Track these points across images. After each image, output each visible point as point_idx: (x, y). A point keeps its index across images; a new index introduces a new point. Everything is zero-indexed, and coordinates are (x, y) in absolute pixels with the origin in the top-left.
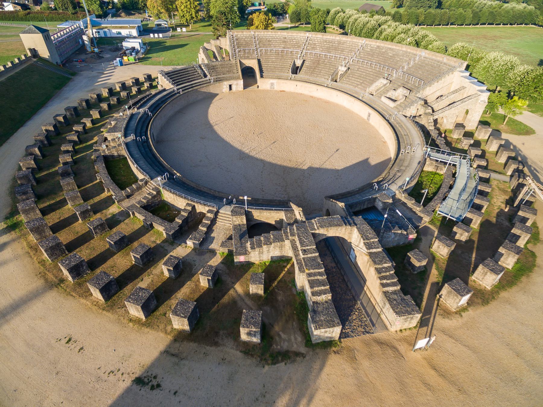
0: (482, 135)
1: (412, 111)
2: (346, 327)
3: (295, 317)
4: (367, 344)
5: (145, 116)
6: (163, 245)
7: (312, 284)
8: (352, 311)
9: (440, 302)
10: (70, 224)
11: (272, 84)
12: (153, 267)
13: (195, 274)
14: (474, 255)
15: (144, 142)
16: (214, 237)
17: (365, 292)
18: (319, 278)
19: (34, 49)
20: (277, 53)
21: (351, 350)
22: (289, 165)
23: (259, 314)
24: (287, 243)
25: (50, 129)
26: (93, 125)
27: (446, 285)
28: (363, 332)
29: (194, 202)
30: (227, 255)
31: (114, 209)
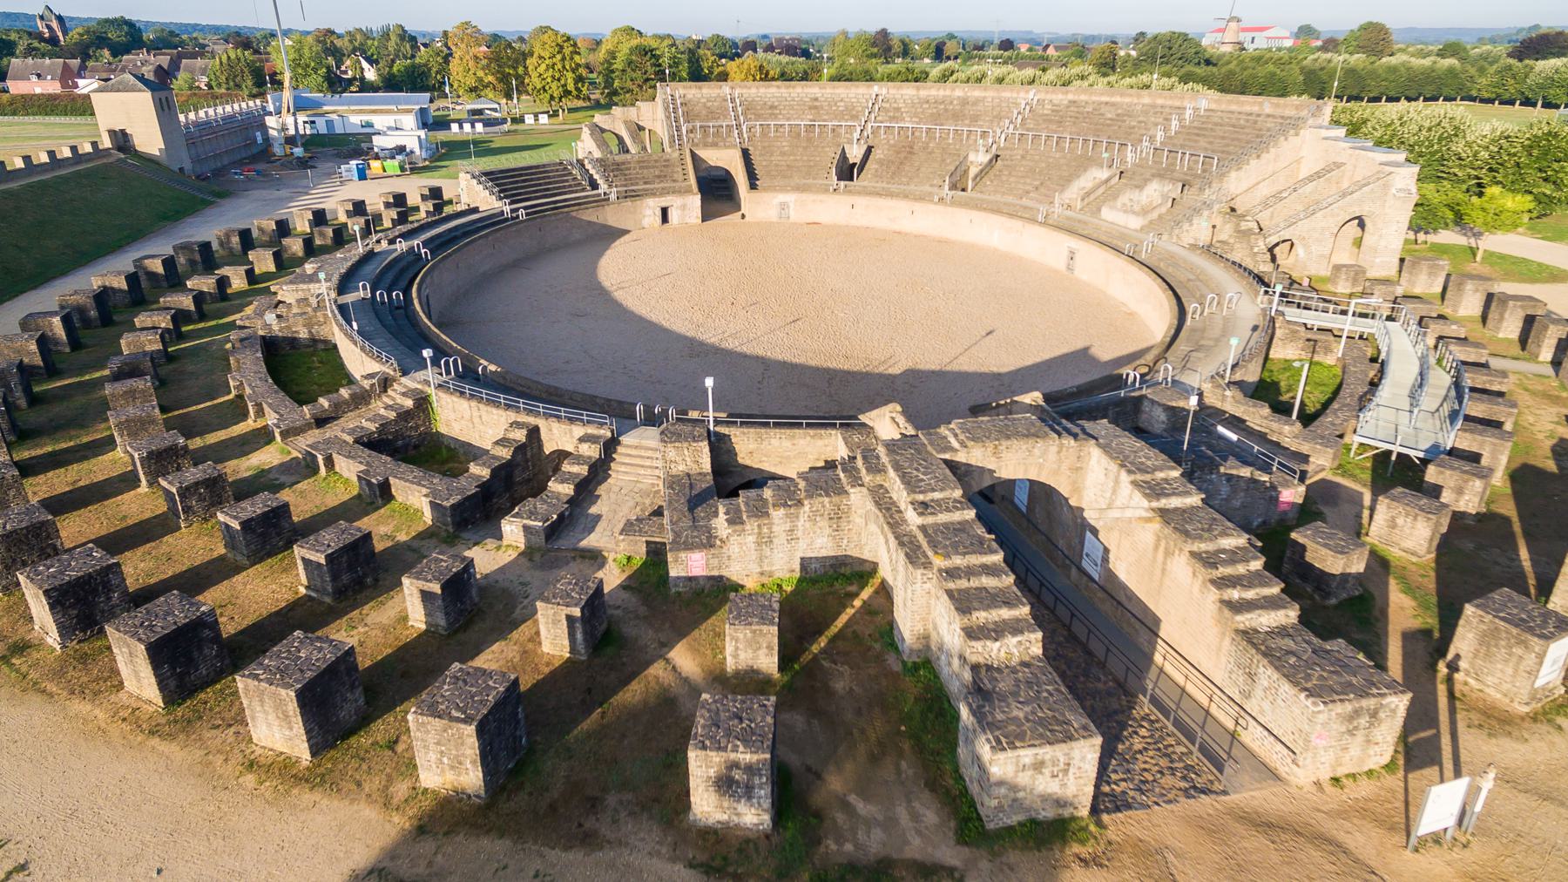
1: (1199, 230)
2: (1114, 776)
3: (906, 746)
4: (1210, 829)
5: (411, 258)
6: (415, 544)
7: (963, 602)
8: (1124, 726)
9: (1458, 688)
10: (107, 497)
12: (371, 604)
13: (525, 621)
14: (1524, 554)
15: (397, 308)
16: (598, 517)
17: (1161, 670)
18: (988, 582)
19: (123, 131)
20: (795, 132)
21: (1147, 853)
23: (765, 706)
24: (859, 500)
25: (115, 285)
26: (250, 284)
27: (1469, 609)
28: (1186, 791)
29: (537, 414)
30: (644, 563)
31: (267, 457)
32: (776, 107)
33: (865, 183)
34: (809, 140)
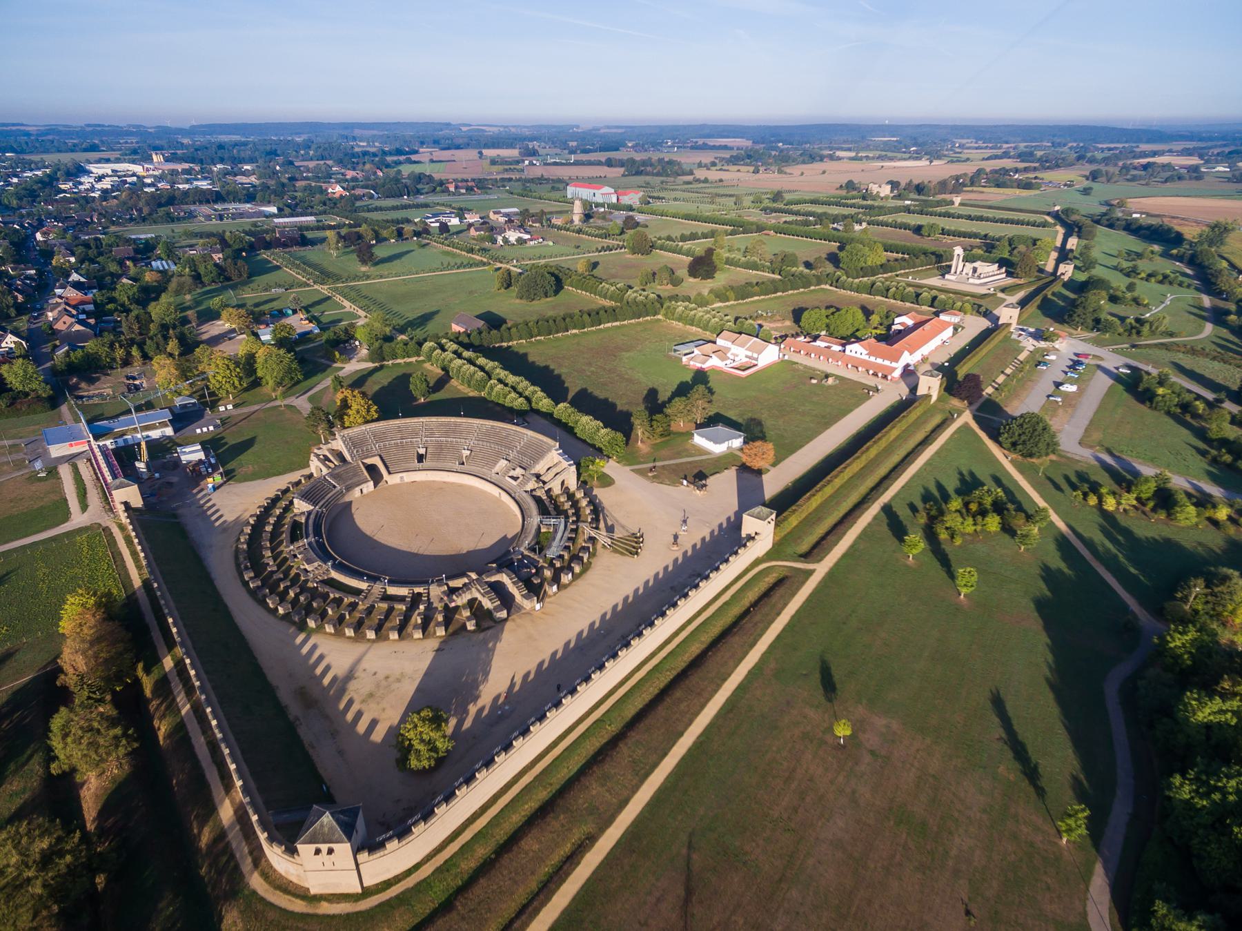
0: (579, 495)
1: (529, 487)
11: (402, 478)
22: (453, 553)
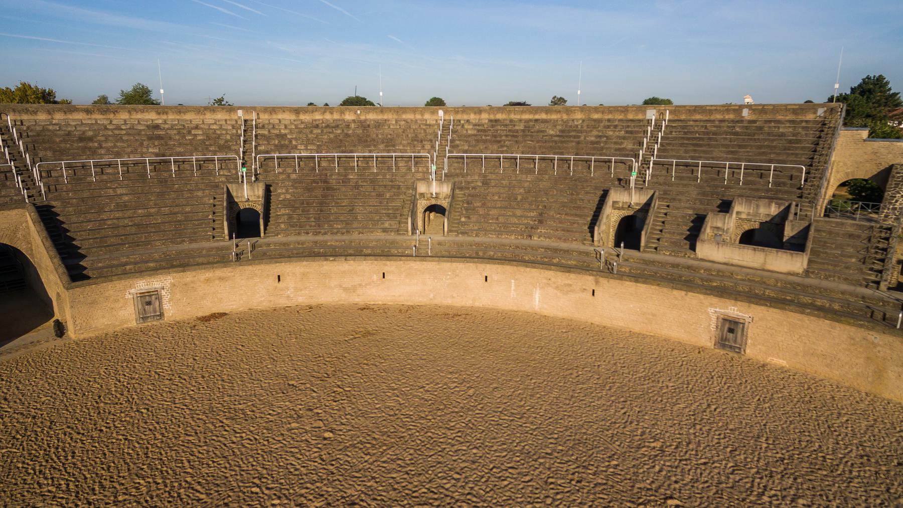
11: (149, 300)
32: (91, 139)
33: (281, 238)
34: (163, 182)
